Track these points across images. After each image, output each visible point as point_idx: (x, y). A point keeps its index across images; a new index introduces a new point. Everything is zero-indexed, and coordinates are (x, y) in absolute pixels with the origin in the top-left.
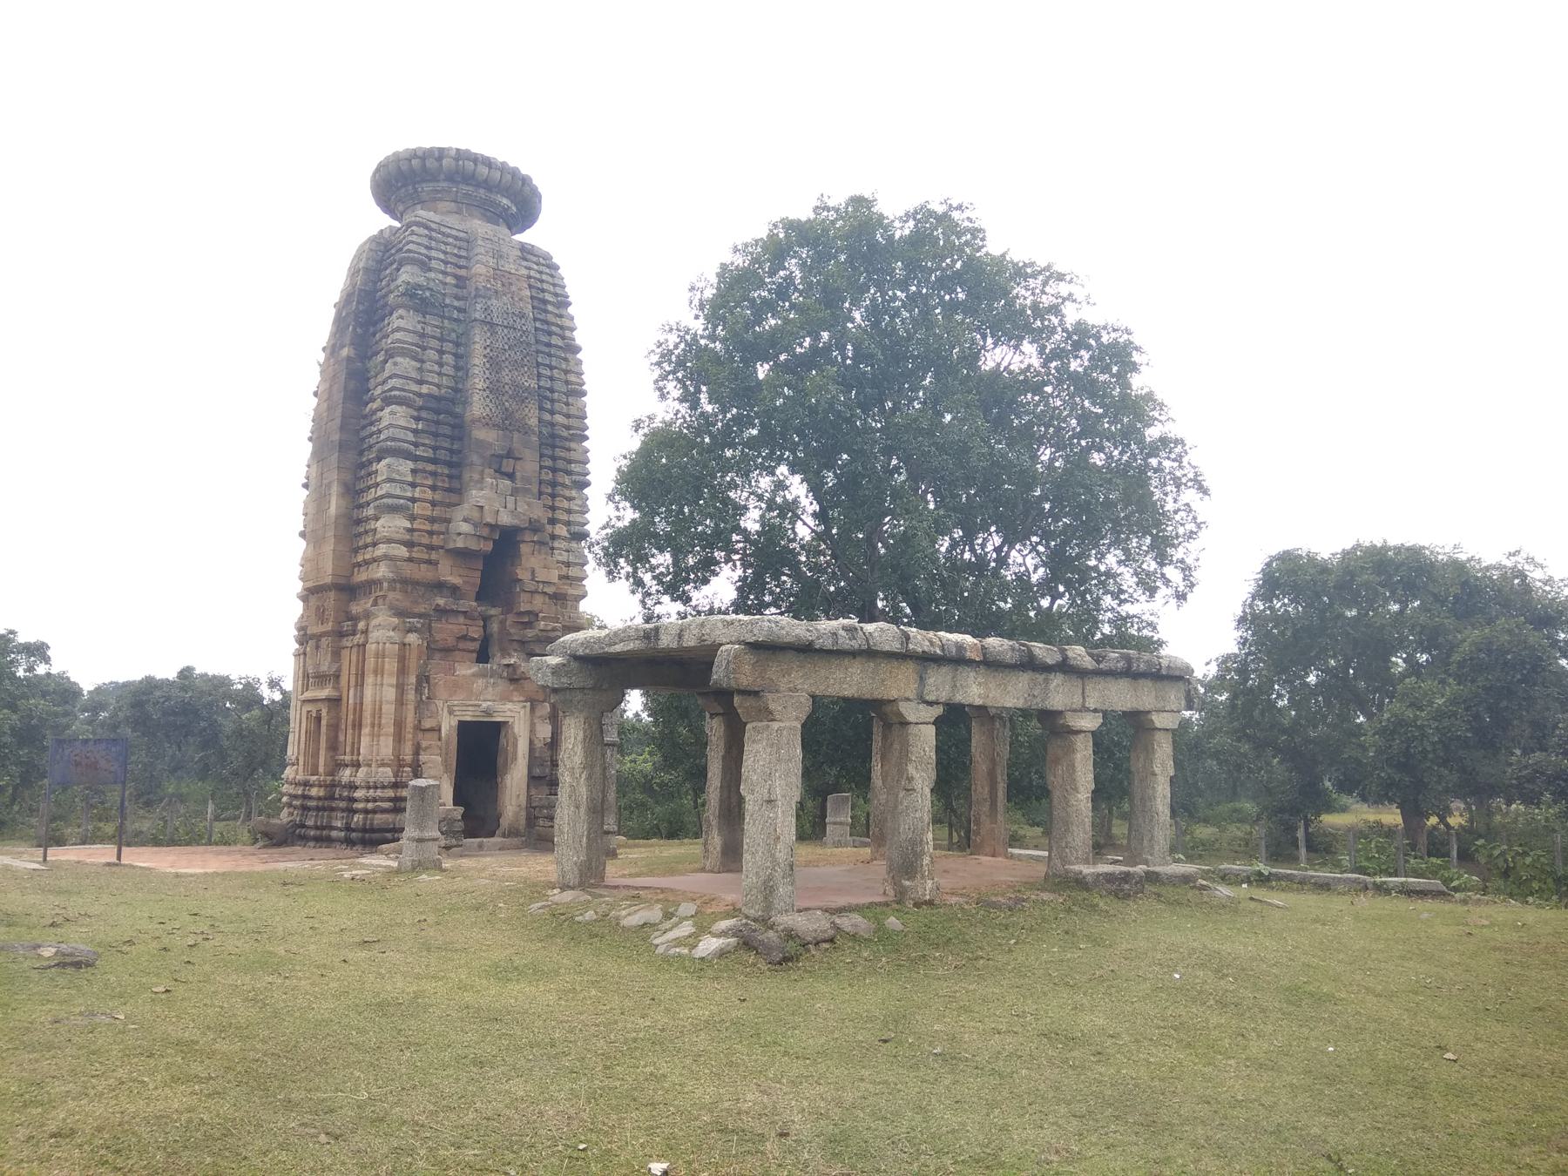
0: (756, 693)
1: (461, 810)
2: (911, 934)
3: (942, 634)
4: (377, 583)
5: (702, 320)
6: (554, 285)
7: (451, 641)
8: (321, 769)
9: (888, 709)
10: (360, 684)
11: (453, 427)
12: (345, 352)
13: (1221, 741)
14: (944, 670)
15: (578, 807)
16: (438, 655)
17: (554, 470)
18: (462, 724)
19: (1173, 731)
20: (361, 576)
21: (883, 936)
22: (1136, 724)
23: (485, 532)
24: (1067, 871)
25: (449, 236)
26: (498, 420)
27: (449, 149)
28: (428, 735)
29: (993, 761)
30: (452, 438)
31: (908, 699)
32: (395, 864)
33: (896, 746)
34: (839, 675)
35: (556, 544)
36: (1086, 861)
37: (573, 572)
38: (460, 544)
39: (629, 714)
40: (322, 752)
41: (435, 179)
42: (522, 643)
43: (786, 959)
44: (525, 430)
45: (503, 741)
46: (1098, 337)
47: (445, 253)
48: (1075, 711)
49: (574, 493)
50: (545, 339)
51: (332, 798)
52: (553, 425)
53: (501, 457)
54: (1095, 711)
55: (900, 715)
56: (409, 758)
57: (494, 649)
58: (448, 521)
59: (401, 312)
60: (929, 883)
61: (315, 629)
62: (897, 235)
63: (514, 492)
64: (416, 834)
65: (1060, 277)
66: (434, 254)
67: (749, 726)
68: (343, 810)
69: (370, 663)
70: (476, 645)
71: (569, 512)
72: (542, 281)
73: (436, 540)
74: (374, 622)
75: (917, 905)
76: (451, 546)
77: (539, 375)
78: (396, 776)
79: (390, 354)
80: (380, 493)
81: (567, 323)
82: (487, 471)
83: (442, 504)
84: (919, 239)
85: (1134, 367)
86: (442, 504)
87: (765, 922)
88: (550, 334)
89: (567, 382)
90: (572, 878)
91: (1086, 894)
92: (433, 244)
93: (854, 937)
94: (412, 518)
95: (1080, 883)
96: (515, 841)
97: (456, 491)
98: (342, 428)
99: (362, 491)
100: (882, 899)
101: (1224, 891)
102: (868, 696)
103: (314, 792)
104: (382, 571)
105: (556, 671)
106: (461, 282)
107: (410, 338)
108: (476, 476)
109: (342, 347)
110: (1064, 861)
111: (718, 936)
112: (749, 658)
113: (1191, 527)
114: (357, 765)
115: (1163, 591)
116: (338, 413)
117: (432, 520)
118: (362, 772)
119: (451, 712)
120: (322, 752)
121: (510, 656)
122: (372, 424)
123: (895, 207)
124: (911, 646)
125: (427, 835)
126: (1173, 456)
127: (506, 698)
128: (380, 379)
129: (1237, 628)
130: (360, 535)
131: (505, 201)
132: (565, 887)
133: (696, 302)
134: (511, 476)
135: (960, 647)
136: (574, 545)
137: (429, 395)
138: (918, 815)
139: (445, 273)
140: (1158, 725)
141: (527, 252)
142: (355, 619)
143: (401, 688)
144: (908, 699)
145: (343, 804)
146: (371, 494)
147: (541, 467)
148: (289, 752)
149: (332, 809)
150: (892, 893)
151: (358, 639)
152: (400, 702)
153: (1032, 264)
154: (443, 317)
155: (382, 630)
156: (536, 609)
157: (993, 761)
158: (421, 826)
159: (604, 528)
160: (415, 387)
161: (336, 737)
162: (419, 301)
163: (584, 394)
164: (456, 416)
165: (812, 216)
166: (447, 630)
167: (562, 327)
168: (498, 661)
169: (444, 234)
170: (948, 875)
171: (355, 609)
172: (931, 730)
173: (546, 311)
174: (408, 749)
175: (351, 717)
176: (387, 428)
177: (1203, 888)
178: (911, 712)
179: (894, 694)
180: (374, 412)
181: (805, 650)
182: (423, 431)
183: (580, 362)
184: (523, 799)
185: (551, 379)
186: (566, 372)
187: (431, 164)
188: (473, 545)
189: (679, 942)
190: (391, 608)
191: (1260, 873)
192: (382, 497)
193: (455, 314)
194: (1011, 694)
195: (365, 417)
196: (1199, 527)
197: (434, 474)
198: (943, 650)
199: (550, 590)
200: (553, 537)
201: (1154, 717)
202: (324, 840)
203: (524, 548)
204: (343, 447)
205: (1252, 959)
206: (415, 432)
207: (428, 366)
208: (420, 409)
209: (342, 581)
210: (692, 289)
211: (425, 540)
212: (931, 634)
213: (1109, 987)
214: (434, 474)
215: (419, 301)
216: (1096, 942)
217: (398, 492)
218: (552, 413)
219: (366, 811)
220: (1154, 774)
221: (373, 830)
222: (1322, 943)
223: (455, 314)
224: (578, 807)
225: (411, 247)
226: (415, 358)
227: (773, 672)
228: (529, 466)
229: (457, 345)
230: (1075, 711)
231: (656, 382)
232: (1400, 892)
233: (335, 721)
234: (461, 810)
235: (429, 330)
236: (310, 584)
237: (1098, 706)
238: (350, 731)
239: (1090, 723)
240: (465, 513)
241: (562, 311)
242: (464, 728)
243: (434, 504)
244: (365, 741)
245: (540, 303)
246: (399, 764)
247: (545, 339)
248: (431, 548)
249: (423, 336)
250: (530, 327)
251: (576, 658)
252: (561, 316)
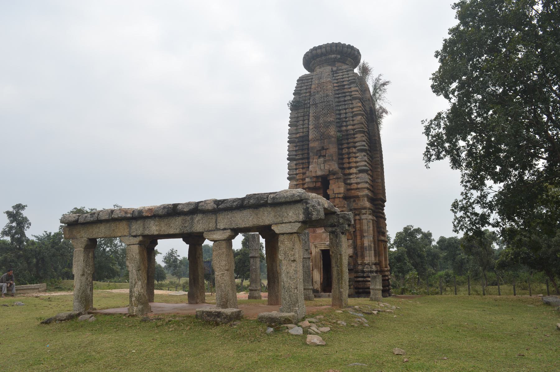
6: (348, 77)
14: (139, 222)
17: (348, 148)
23: (314, 179)
31: (125, 236)
44: (329, 137)
52: (347, 131)
53: (320, 150)
63: (325, 162)
71: (356, 162)
82: (315, 157)
88: (345, 96)
89: (353, 112)
119: (316, 247)
131: (333, 56)
137: (300, 137)
139: (306, 93)
144: (125, 236)
167: (351, 92)
169: (308, 79)
186: (352, 108)
188: (311, 185)
197: (303, 163)
203: (331, 182)
206: (296, 151)
208: (298, 142)
235: (299, 115)
237: (227, 227)
247: (342, 99)
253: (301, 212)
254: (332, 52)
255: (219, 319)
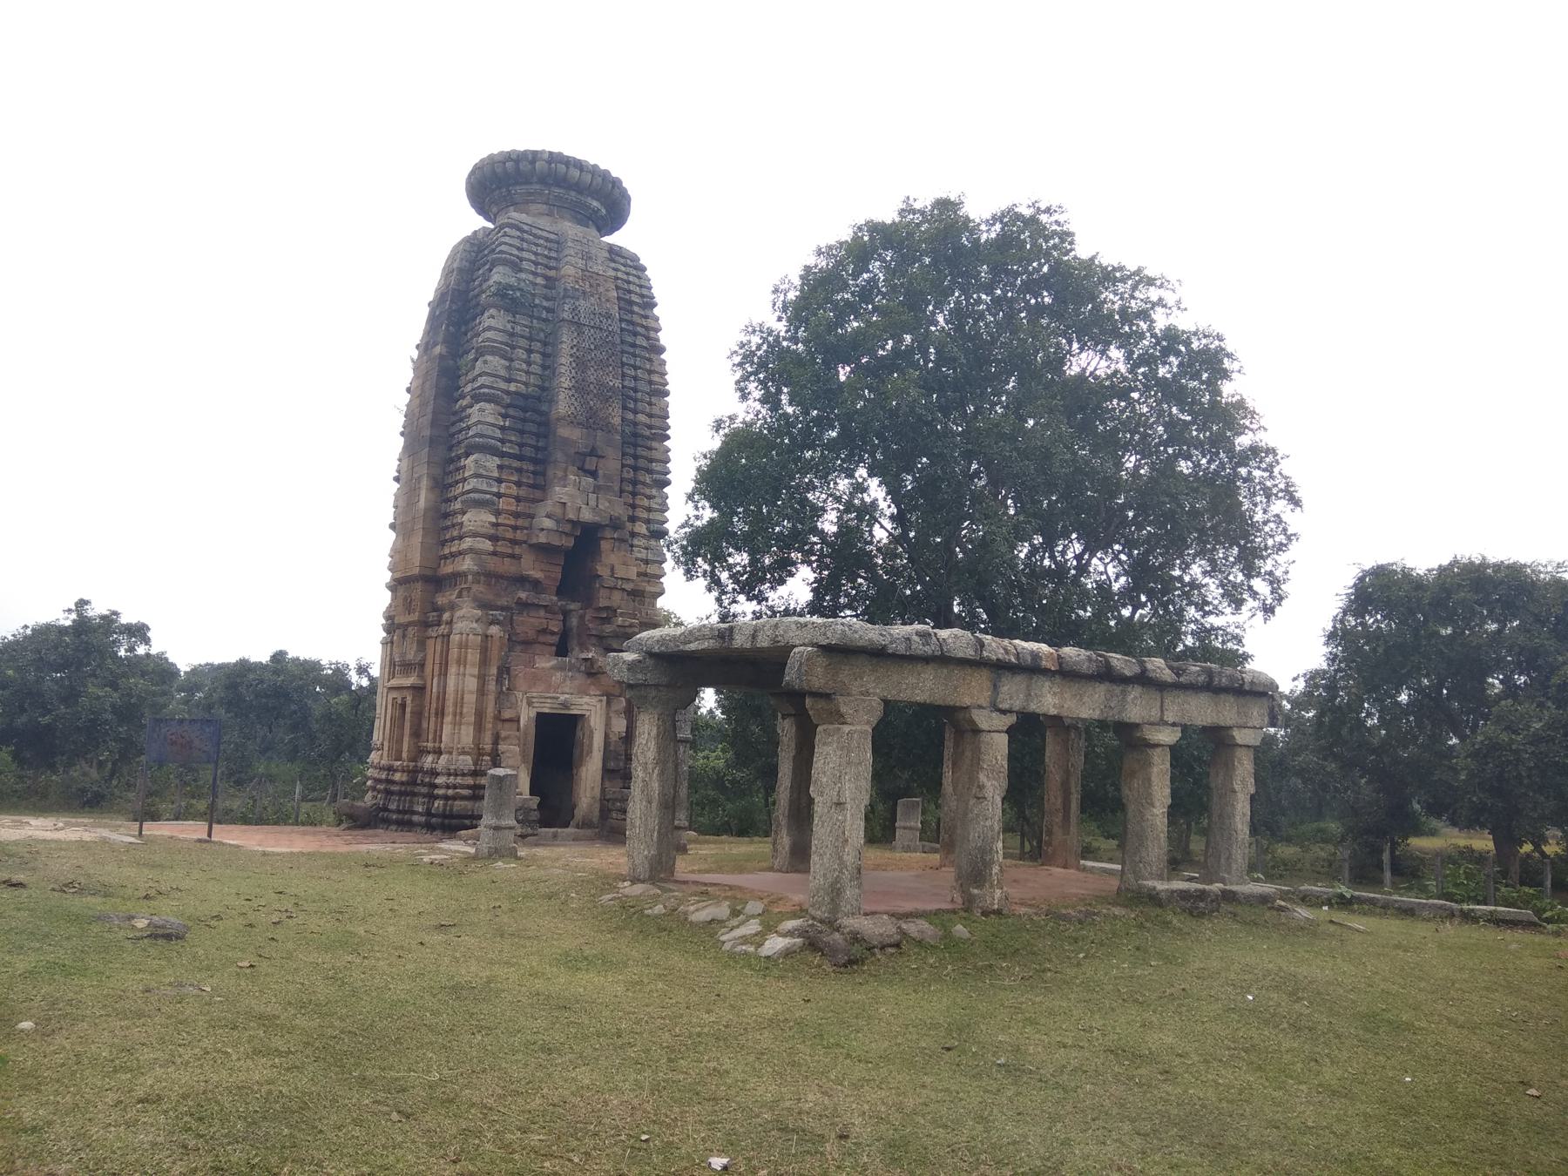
0: (827, 697)
1: (537, 799)
2: (977, 943)
3: (1017, 642)
4: (463, 575)
5: (784, 322)
6: (641, 286)
7: (531, 634)
8: (404, 755)
9: (961, 715)
10: (444, 673)
11: (540, 424)
12: (438, 350)
13: (1307, 758)
14: (1018, 678)
15: (650, 802)
16: (519, 648)
17: (635, 469)
18: (541, 717)
19: (1255, 748)
20: (448, 569)
21: (950, 944)
22: (1217, 739)
23: (568, 527)
24: (1140, 887)
25: (540, 237)
26: (582, 419)
27: (543, 152)
28: (507, 725)
29: (1067, 772)
30: (538, 436)
31: (980, 707)
32: (472, 850)
33: (968, 754)
34: (912, 680)
35: (636, 542)
36: (1160, 878)
37: (651, 569)
38: (542, 539)
39: (704, 711)
40: (406, 739)
41: (528, 182)
42: (600, 638)
43: (851, 962)
44: (608, 428)
45: (579, 733)
46: (1188, 343)
47: (536, 254)
48: (1152, 724)
49: (654, 492)
50: (630, 339)
51: (414, 783)
52: (635, 424)
53: (585, 455)
54: (1174, 725)
55: (973, 722)
56: (488, 747)
57: (573, 644)
58: (532, 516)
59: (492, 311)
60: (998, 893)
61: (402, 619)
62: (984, 237)
64: (493, 822)
65: (1150, 282)
66: (525, 255)
67: (819, 729)
68: (424, 796)
69: (454, 653)
70: (556, 639)
71: (649, 510)
72: (629, 282)
73: (519, 535)
74: (459, 613)
75: (985, 913)
76: (534, 541)
77: (624, 375)
78: (475, 764)
79: (481, 353)
80: (467, 487)
81: (651, 323)
82: (571, 468)
83: (527, 500)
84: (1006, 242)
85: (1225, 375)
86: (527, 500)
87: (832, 924)
88: (635, 334)
89: (651, 382)
90: (642, 870)
91: (1159, 911)
92: (525, 245)
93: (919, 943)
94: (497, 513)
95: (1154, 899)
96: (589, 832)
97: (540, 487)
98: (434, 423)
99: (451, 486)
100: (950, 906)
101: (1303, 912)
102: (940, 702)
103: (397, 777)
104: (467, 564)
105: (632, 666)
106: (551, 282)
107: (500, 337)
108: (560, 474)
109: (435, 344)
110: (1138, 876)
111: (784, 935)
112: (822, 661)
113: (1280, 538)
114: (439, 752)
115: (1251, 603)
116: (430, 409)
117: (517, 515)
118: (444, 758)
119: (530, 704)
120: (406, 739)
121: (588, 650)
122: (461, 420)
123: (980, 209)
124: (985, 654)
125: (503, 823)
126: (1264, 465)
127: (583, 692)
128: (470, 376)
129: (1327, 644)
130: (447, 528)
131: (595, 204)
132: (635, 880)
133: (779, 304)
134: (594, 474)
135: (1035, 656)
136: (653, 542)
137: (516, 393)
138: (988, 823)
139: (535, 274)
140: (1239, 741)
141: (615, 253)
142: (440, 610)
143: (482, 678)
144: (980, 707)
145: (424, 790)
146: (459, 489)
147: (623, 466)
148: (375, 737)
149: (414, 794)
150: (960, 900)
151: (443, 629)
152: (481, 692)
153: (1121, 269)
154: (532, 317)
155: (466, 621)
156: (615, 605)
157: (1067, 772)
158: (498, 816)
159: (682, 526)
160: (503, 385)
161: (420, 724)
162: (509, 301)
163: (667, 394)
164: (541, 413)
165: (897, 219)
166: (528, 624)
167: (647, 328)
168: (578, 655)
169: (535, 236)
170: (1018, 885)
171: (441, 600)
172: (1004, 738)
173: (632, 312)
174: (488, 738)
175: (434, 705)
176: (476, 424)
177: (1281, 909)
178: (983, 719)
179: (967, 701)
180: (464, 409)
181: (878, 655)
182: (509, 428)
183: (663, 363)
184: (597, 792)
185: (635, 378)
186: (650, 372)
187: (525, 167)
188: (556, 541)
189: (745, 940)
190: (475, 599)
191: (1342, 896)
192: (469, 492)
193: (544, 315)
194: (1087, 705)
195: (455, 413)
196: (1289, 538)
197: (519, 470)
198: (1018, 657)
199: (629, 587)
200: (633, 535)
201: (1236, 733)
202: (405, 825)
203: (605, 545)
204: (432, 442)
205: (1329, 983)
206: (502, 428)
207: (516, 364)
208: (508, 406)
209: (429, 573)
210: (776, 291)
211: (509, 535)
212: (1006, 642)
213: (1180, 1006)
214: (519, 470)
215: (509, 301)
216: (1168, 960)
217: (484, 487)
218: (635, 412)
219: (446, 798)
220: (1234, 791)
221: (452, 816)
222: (1403, 969)
223: (544, 315)
224: (650, 802)
225: (503, 248)
226: (504, 357)
227: (845, 675)
228: (611, 464)
229: (545, 344)
230: (1152, 724)
231: (738, 382)
232: (1489, 921)
233: (419, 710)
234: (537, 799)
235: (518, 329)
236: (398, 575)
237: (1177, 720)
238: (433, 719)
239: (1168, 736)
240: (549, 509)
241: (648, 312)
242: (545, 722)
243: (518, 499)
244: (447, 729)
245: (626, 304)
246: (478, 752)
247: (630, 339)
248: (514, 542)
249: (512, 335)
250: (615, 327)
251: (651, 654)
252: (646, 317)
253: (1265, 712)
254: (596, 193)
255: (1202, 905)
